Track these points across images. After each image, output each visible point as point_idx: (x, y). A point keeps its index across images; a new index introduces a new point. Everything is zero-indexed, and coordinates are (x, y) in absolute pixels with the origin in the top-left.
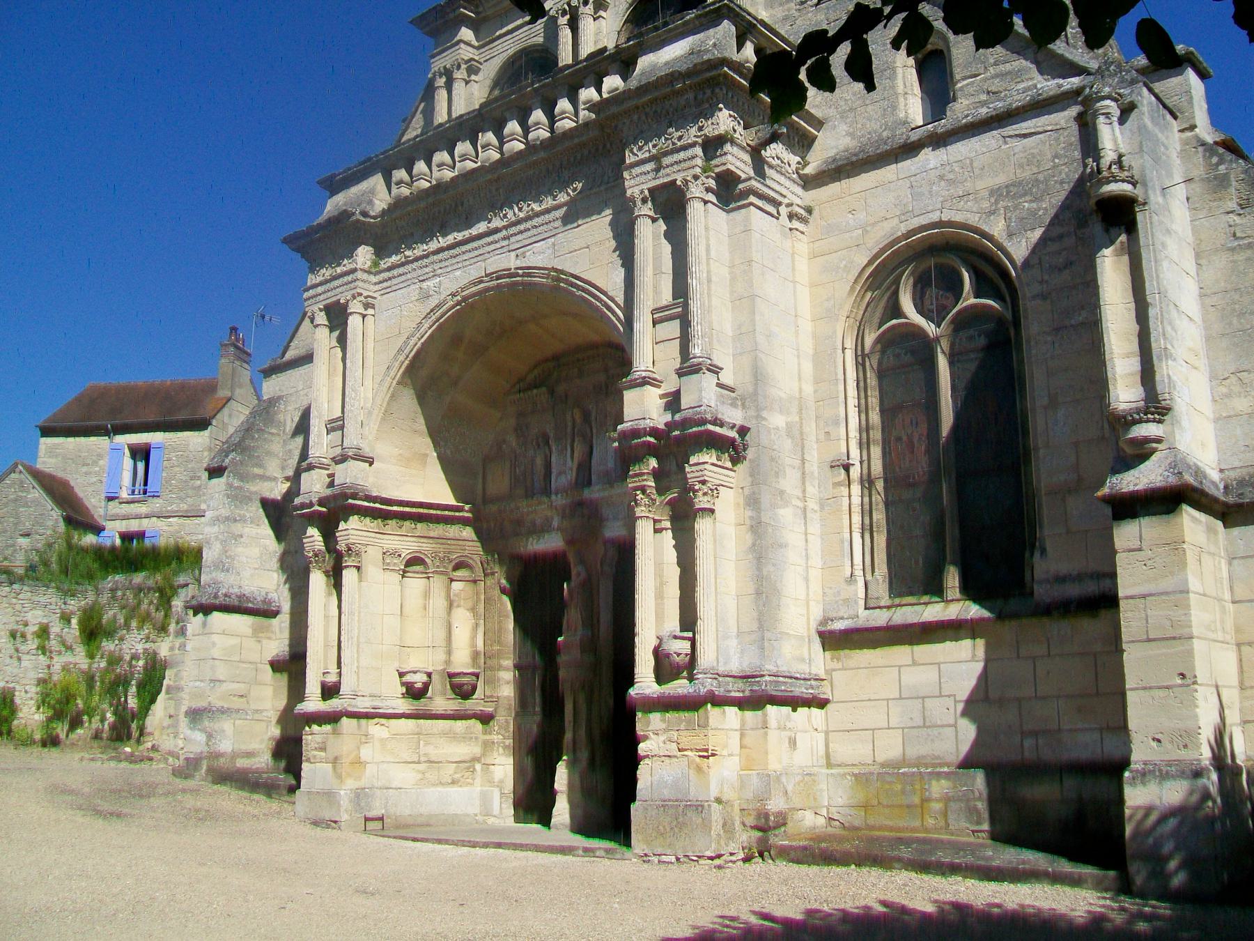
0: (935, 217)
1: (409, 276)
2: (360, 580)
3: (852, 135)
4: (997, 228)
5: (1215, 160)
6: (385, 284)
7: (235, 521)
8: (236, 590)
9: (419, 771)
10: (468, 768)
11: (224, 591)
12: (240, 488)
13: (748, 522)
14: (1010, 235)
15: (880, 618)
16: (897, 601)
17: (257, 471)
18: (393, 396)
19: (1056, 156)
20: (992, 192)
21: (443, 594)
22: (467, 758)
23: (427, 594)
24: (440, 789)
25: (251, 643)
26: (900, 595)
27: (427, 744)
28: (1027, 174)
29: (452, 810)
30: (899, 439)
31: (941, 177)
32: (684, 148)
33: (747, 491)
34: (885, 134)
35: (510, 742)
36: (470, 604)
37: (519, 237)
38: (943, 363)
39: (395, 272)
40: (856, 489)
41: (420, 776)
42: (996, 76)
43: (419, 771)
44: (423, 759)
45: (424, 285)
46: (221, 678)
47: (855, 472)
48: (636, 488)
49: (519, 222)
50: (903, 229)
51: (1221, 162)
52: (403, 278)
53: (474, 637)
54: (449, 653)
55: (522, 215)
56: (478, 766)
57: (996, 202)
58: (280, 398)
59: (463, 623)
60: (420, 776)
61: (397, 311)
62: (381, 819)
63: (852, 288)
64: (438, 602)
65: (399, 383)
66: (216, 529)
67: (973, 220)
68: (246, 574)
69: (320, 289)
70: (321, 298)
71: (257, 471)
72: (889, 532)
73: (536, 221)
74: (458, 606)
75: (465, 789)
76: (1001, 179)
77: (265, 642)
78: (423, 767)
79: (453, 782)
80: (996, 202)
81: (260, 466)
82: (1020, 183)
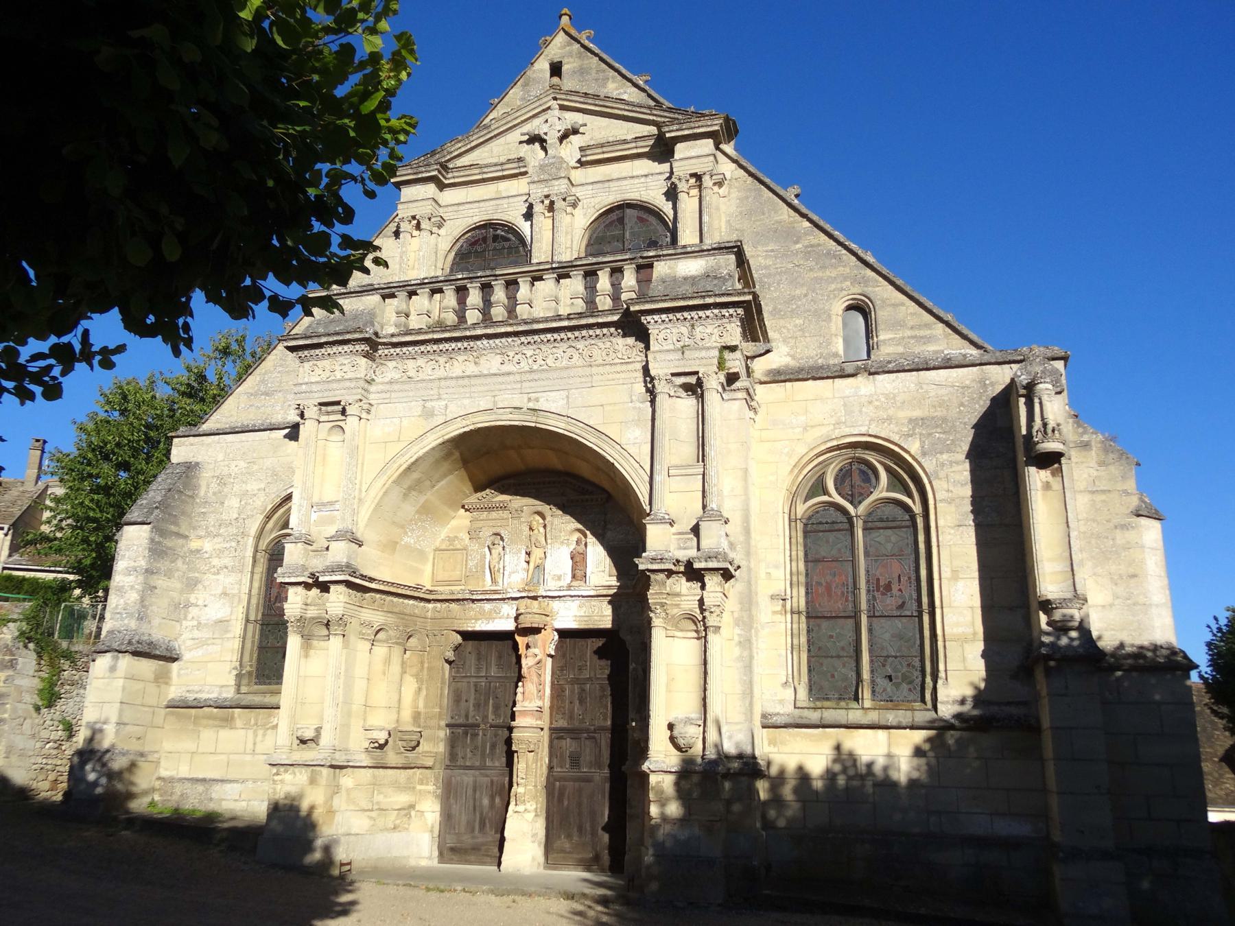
0: (863, 430)
1: (411, 394)
3: (793, 357)
4: (914, 447)
5: (1080, 430)
6: (384, 395)
7: (153, 573)
8: (146, 638)
11: (137, 638)
12: (159, 543)
13: (736, 638)
14: (924, 454)
15: (814, 716)
16: (819, 704)
17: (173, 528)
18: (385, 493)
19: (962, 404)
20: (910, 420)
22: (406, 805)
23: (388, 661)
24: (386, 833)
25: (152, 688)
26: (818, 699)
27: (380, 793)
28: (939, 413)
29: (395, 853)
30: (819, 584)
31: (870, 403)
32: (708, 348)
33: (736, 615)
34: (820, 361)
35: (439, 791)
36: (414, 670)
37: (532, 384)
38: (859, 533)
39: (396, 387)
40: (789, 616)
42: (912, 337)
43: (371, 818)
44: (376, 807)
45: (429, 404)
46: (126, 720)
47: (788, 602)
48: (655, 604)
49: (531, 371)
50: (837, 433)
51: (1085, 433)
52: (405, 394)
53: (415, 700)
54: (399, 712)
55: (535, 367)
56: (413, 813)
57: (914, 429)
58: (197, 464)
59: (410, 685)
61: (397, 421)
62: (349, 864)
63: (792, 471)
64: (396, 668)
65: (394, 482)
66: (132, 578)
67: (896, 438)
68: (156, 622)
69: (314, 388)
70: (316, 395)
71: (173, 528)
72: (809, 651)
73: (550, 375)
75: (404, 834)
76: (917, 413)
77: (163, 686)
78: (374, 814)
80: (914, 429)
81: (176, 524)
82: (933, 418)
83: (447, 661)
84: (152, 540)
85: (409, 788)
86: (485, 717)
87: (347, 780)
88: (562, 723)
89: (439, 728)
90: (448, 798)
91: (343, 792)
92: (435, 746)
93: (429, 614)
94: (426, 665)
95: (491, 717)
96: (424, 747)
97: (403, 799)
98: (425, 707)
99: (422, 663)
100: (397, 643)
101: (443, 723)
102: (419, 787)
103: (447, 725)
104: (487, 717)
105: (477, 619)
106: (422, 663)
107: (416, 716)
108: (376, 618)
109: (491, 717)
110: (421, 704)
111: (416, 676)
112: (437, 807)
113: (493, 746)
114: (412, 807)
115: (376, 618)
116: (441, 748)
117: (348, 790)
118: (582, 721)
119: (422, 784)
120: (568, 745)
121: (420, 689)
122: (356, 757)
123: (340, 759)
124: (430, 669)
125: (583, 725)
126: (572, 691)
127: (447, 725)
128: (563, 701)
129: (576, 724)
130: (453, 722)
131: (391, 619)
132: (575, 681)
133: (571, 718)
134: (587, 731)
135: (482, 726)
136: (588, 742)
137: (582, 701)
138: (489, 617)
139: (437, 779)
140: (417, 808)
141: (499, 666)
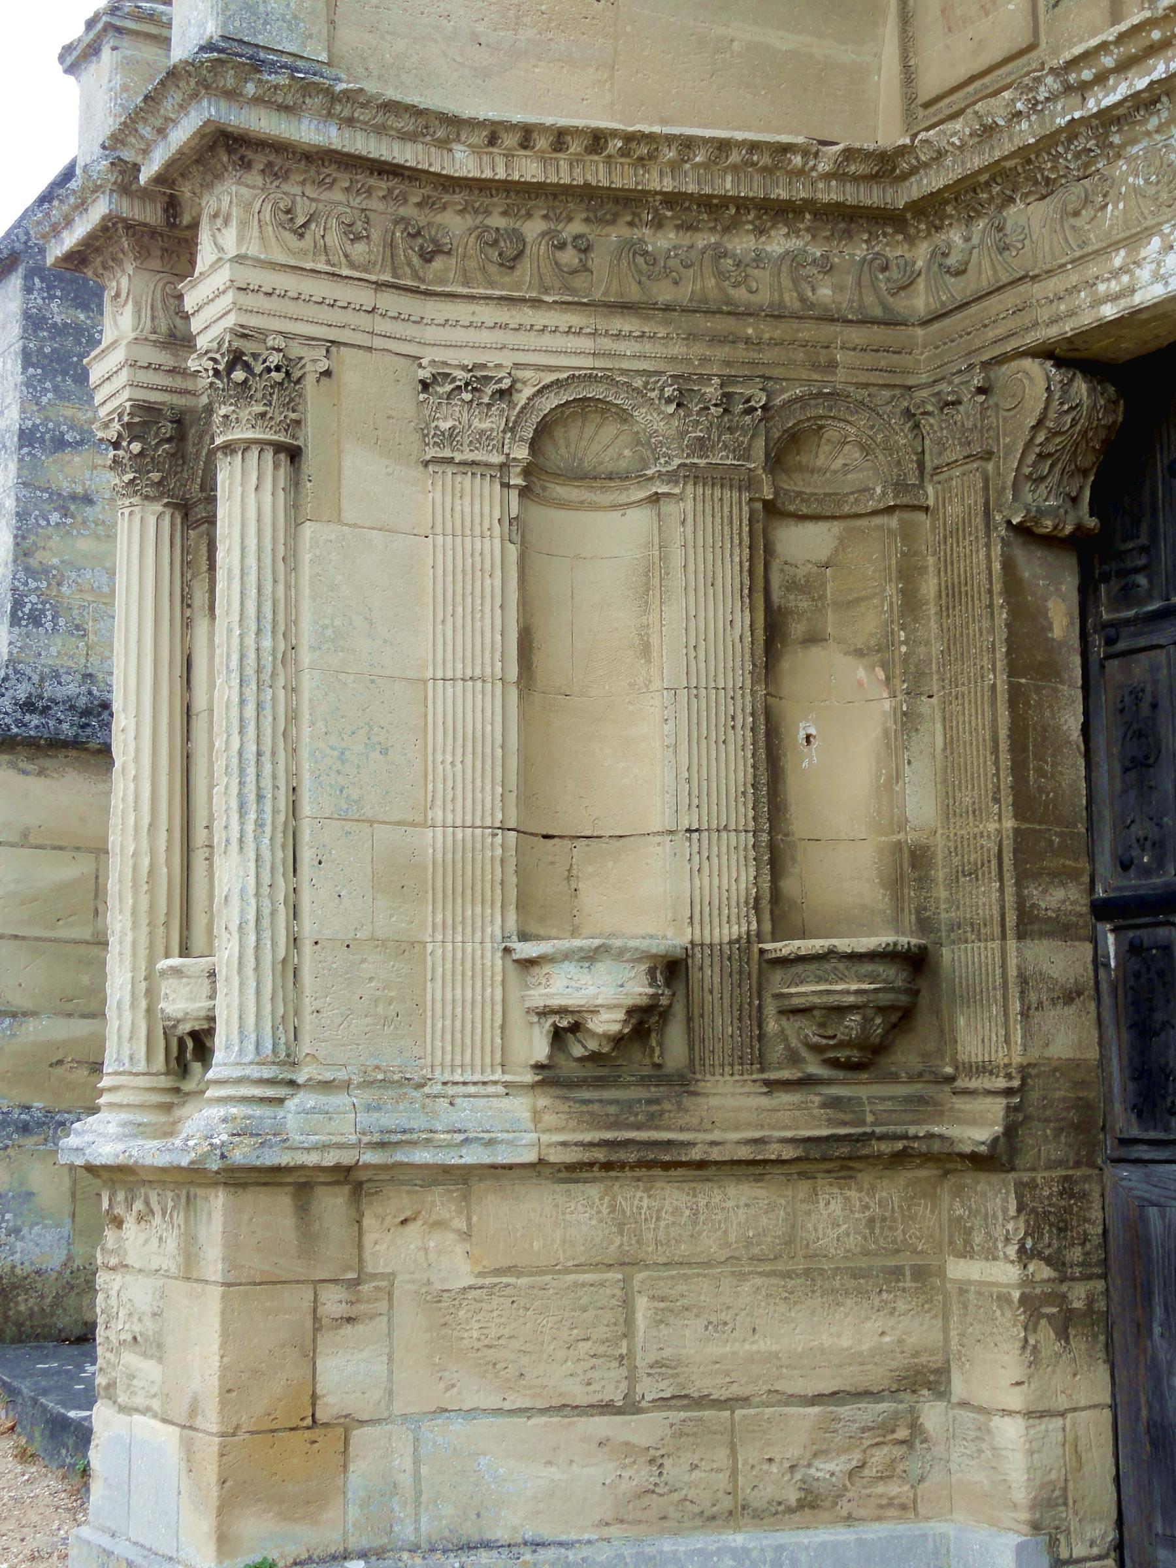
2: (295, 515)
7: (60, 444)
9: (628, 1450)
10: (886, 1427)
21: (730, 574)
22: (877, 1376)
27: (669, 1310)
36: (869, 623)
41: (642, 1475)
44: (649, 1389)
53: (890, 784)
56: (932, 1415)
60: (642, 1475)
74: (814, 639)
78: (645, 1430)
79: (811, 1503)
83: (1024, 532)
84: (33, 322)
85: (906, 1275)
87: (417, 1251)
89: (1029, 924)
90: (1142, 1329)
91: (409, 1318)
92: (1023, 1018)
93: (920, 301)
94: (929, 586)
96: (984, 1037)
97: (856, 1335)
98: (948, 813)
99: (908, 575)
100: (694, 475)
101: (1061, 898)
102: (959, 1269)
103: (1102, 910)
105: (1133, 240)
106: (908, 575)
107: (911, 865)
108: (540, 345)
110: (921, 807)
111: (879, 652)
112: (1087, 1386)
114: (927, 1378)
115: (540, 345)
116: (1069, 1036)
117: (436, 1301)
119: (966, 1252)
121: (908, 720)
122: (471, 1113)
123: (315, 1128)
124: (952, 595)
127: (1102, 910)
130: (1132, 885)
131: (638, 348)
139: (1049, 1230)
140: (958, 1387)
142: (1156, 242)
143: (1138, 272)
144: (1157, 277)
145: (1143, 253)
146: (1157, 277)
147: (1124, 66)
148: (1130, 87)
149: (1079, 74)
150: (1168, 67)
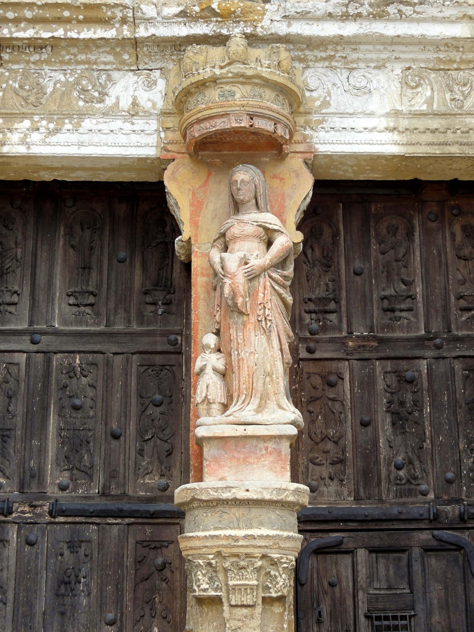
86: (30, 480)
88: (339, 498)
95: (54, 477)
104: (38, 475)
109: (54, 477)
113: (66, 584)
118: (409, 487)
120: (361, 573)
125: (416, 506)
126: (368, 383)
128: (333, 418)
129: (389, 502)
132: (379, 346)
133: (368, 476)
134: (435, 521)
135: (22, 510)
136: (434, 562)
137: (401, 418)
138: (64, 114)
141: (81, 298)
142: (27, 123)
143: (9, 135)
144: (23, 142)
145: (16, 126)
146: (23, 142)
147: (34, 21)
148: (37, 33)
149: (5, 12)
150: (66, 33)
